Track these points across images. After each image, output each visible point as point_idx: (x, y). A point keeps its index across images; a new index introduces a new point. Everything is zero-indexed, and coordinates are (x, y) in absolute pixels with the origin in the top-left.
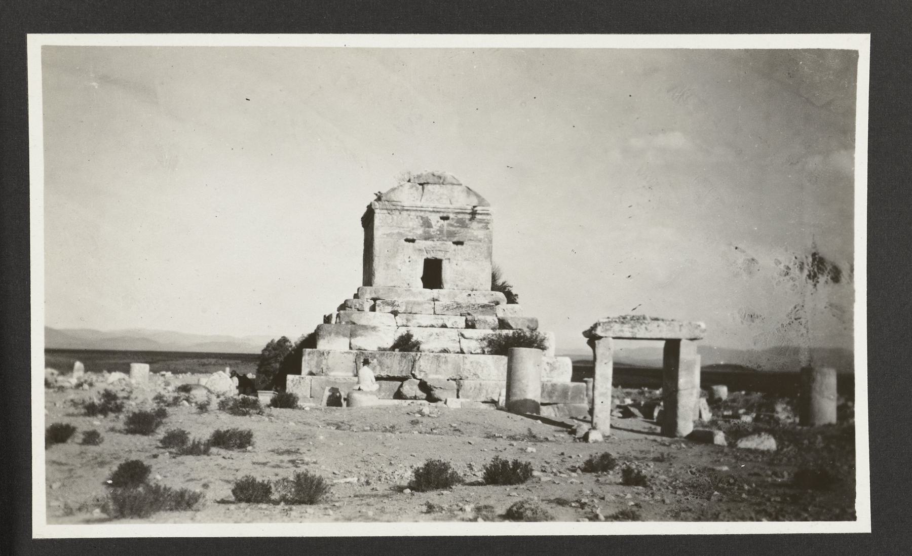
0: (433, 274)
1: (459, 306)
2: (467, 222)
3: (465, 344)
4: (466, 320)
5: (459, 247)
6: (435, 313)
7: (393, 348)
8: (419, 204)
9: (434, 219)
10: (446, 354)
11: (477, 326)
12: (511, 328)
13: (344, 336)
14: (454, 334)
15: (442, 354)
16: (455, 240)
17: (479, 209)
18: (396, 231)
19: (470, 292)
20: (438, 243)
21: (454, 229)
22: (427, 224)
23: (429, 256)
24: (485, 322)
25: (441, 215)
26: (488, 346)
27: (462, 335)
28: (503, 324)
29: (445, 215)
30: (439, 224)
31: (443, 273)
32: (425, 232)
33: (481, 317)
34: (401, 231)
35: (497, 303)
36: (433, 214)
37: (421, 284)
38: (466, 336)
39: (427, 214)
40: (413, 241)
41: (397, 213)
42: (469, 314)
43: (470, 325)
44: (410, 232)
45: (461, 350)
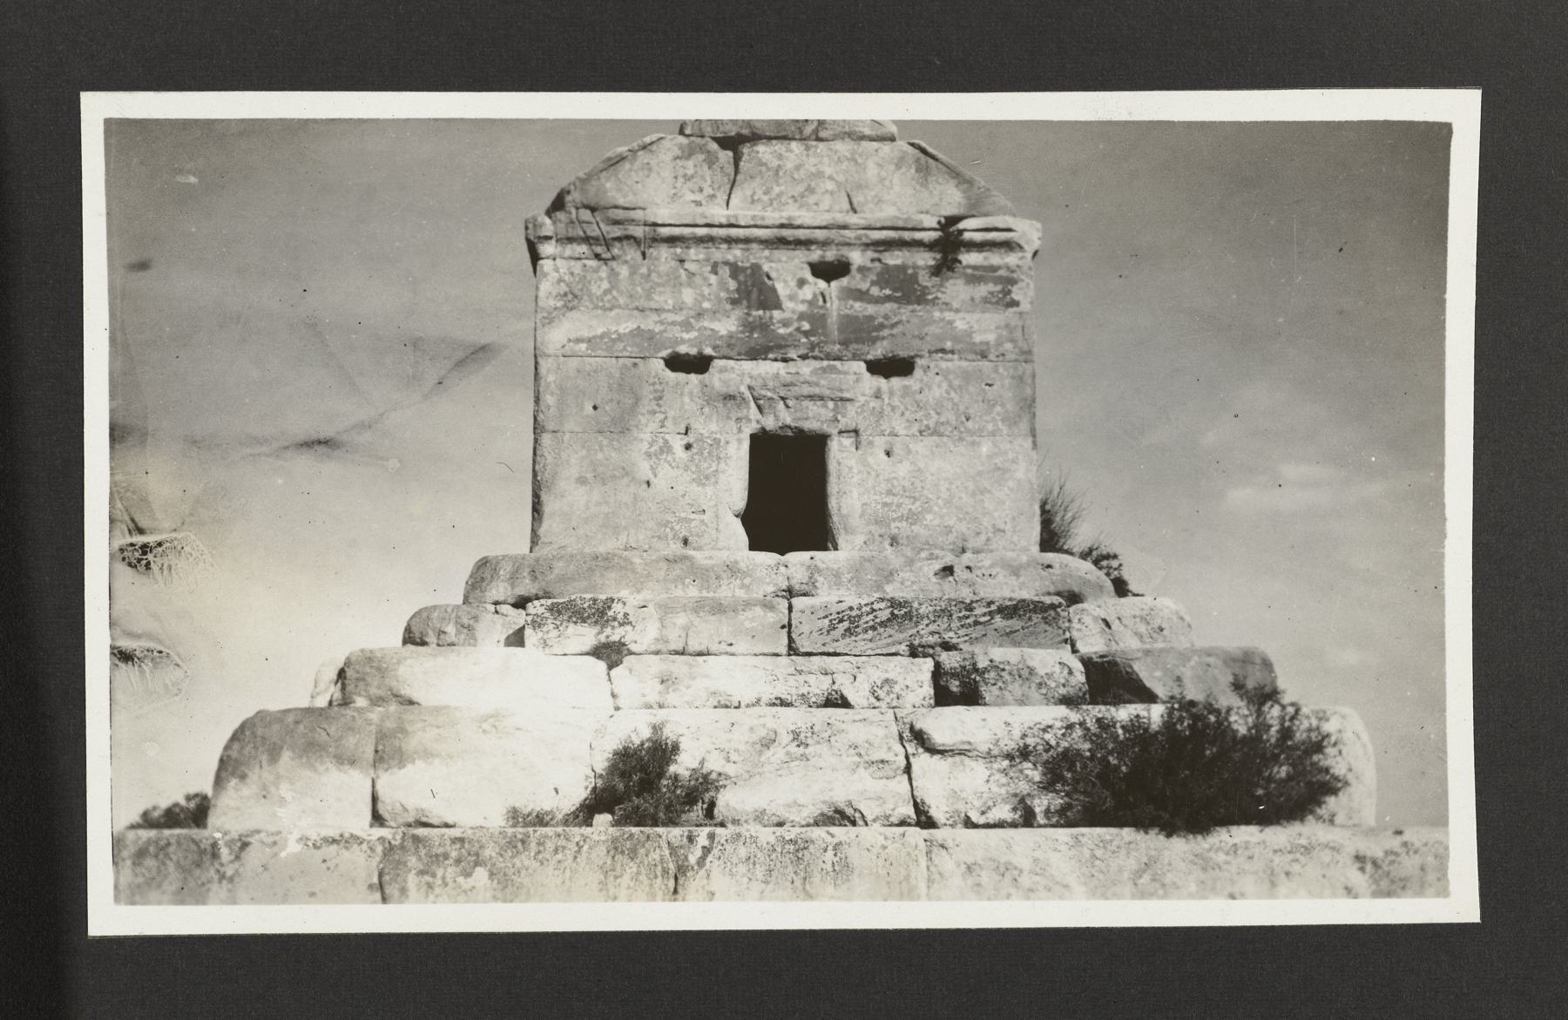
0: (788, 497)
1: (901, 613)
2: (925, 279)
3: (937, 782)
4: (938, 673)
5: (896, 382)
6: (792, 650)
7: (586, 812)
8: (718, 213)
9: (788, 274)
10: (841, 833)
11: (988, 692)
12: (1149, 697)
13: (346, 760)
14: (880, 736)
15: (819, 833)
16: (878, 352)
17: (971, 228)
18: (626, 327)
19: (949, 559)
20: (806, 368)
21: (871, 309)
22: (755, 291)
23: (770, 423)
24: (1026, 674)
25: (816, 255)
26: (1047, 786)
27: (920, 737)
28: (1108, 680)
29: (831, 255)
30: (807, 293)
31: (833, 487)
32: (749, 326)
33: (1002, 654)
34: (650, 323)
35: (1074, 598)
36: (782, 254)
37: (742, 537)
38: (939, 737)
39: (760, 256)
40: (697, 364)
41: (632, 254)
42: (947, 646)
43: (960, 689)
44: (686, 325)
45: (920, 808)
